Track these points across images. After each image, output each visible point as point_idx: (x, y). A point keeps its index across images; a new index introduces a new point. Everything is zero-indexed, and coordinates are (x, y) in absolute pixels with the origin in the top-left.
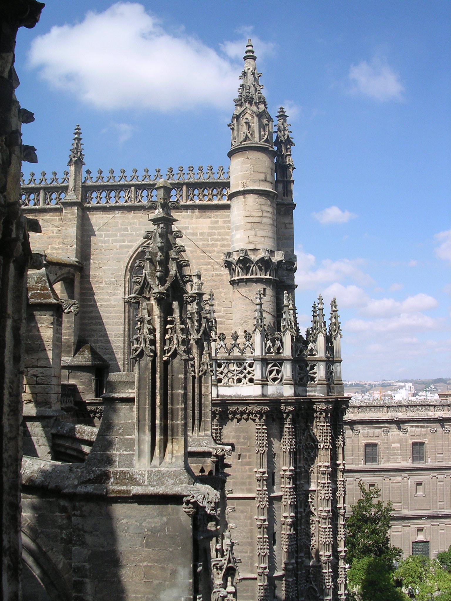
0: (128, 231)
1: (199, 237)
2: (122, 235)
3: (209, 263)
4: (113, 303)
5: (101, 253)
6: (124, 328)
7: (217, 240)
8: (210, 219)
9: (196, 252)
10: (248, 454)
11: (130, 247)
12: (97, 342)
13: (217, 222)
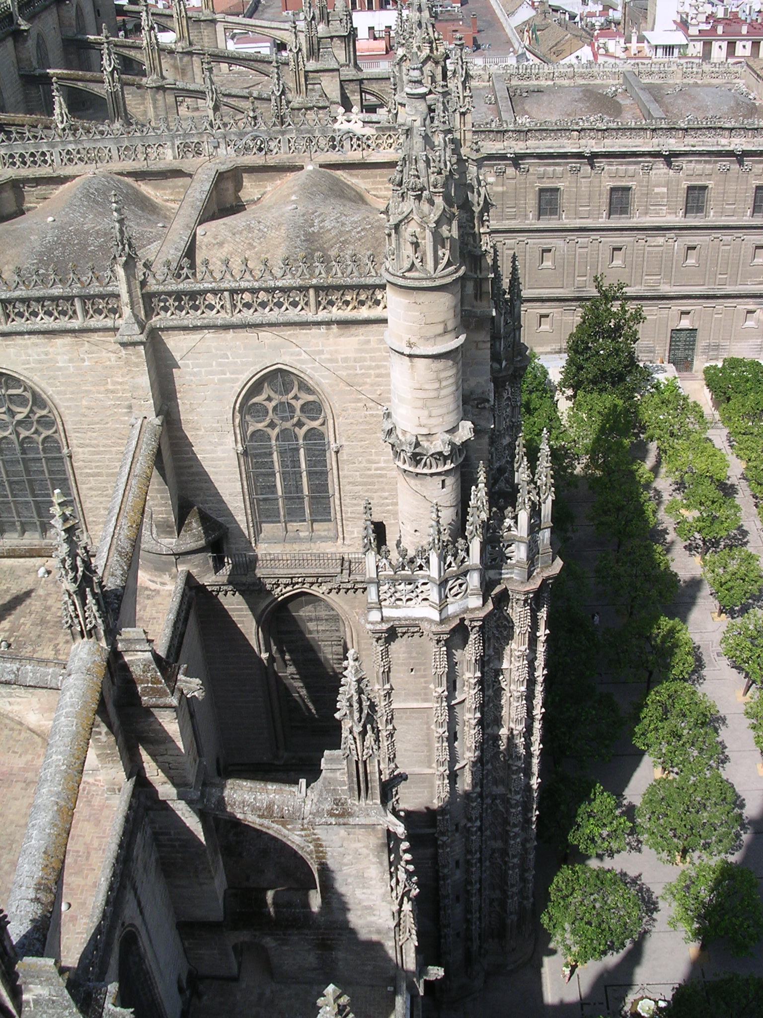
0: (228, 358)
1: (340, 364)
2: (219, 364)
3: (359, 400)
4: (220, 454)
5: (191, 390)
6: (242, 484)
7: (370, 368)
8: (357, 338)
9: (338, 385)
10: (423, 668)
11: (234, 381)
12: (206, 502)
13: (368, 342)
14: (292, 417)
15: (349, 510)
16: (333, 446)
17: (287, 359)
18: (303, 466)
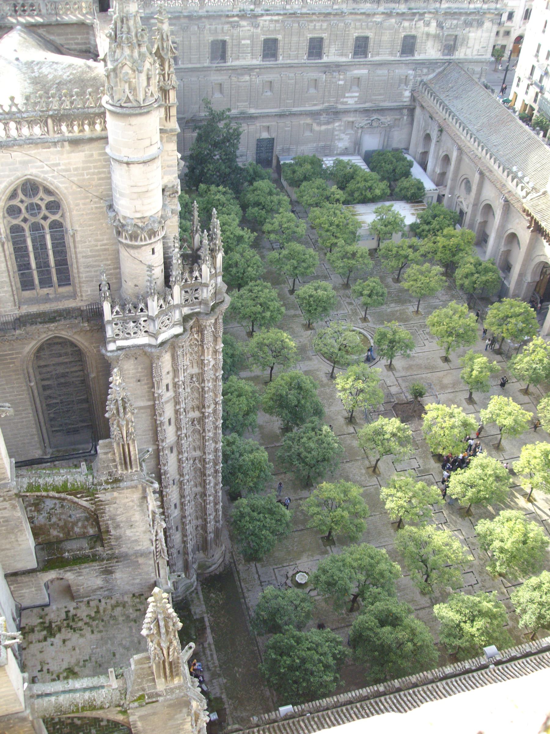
1: (72, 172)
3: (87, 198)
7: (94, 174)
13: (92, 155)
14: (39, 213)
15: (84, 275)
16: (71, 232)
17: (34, 171)
18: (49, 246)
